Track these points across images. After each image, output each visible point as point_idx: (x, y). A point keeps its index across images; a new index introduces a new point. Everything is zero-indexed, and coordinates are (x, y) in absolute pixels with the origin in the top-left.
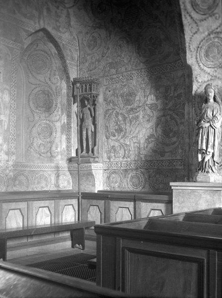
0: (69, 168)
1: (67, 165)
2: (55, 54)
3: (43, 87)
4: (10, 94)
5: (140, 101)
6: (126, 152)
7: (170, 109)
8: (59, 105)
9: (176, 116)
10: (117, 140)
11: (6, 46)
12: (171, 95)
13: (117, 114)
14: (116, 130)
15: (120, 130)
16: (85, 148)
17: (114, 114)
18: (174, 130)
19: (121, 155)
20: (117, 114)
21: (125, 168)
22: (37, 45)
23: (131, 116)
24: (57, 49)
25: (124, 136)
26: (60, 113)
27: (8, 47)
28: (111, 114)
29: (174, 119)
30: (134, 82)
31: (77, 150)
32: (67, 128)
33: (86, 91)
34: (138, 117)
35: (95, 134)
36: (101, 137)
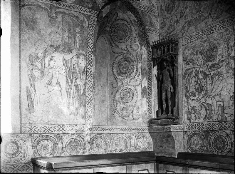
0: (149, 130)
1: (147, 127)
2: (135, 21)
3: (125, 55)
4: (86, 59)
5: (222, 54)
6: (208, 112)
8: (140, 70)
10: (198, 100)
11: (83, 14)
14: (196, 89)
15: (200, 90)
16: (165, 109)
17: (194, 73)
22: (118, 15)
23: (212, 73)
24: (136, 16)
25: (205, 95)
26: (140, 77)
27: (84, 15)
28: (190, 74)
30: (215, 35)
31: (157, 112)
32: (146, 92)
33: (164, 52)
34: (220, 74)
35: (174, 95)
36: (181, 96)
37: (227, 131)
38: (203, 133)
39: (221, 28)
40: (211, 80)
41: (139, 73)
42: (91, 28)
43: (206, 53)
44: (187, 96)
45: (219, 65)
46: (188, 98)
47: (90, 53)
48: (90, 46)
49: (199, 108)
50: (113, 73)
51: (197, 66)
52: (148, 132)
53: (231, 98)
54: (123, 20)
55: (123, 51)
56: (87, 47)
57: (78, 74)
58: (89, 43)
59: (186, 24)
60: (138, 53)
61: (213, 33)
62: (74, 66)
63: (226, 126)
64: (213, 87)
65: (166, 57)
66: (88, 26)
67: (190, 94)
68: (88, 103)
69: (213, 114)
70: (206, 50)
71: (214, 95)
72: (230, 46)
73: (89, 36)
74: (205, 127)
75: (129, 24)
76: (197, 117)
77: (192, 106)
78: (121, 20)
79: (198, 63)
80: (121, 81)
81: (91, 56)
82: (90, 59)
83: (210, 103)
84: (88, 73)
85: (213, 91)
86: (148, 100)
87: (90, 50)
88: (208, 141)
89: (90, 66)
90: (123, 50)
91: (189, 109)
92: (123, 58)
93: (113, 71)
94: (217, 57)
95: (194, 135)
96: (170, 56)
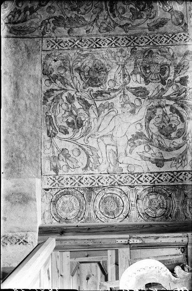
5: (114, 81)
7: (168, 98)
10: (72, 140)
14: (68, 123)
15: (77, 124)
17: (64, 99)
18: (178, 127)
19: (79, 164)
23: (98, 103)
28: (57, 97)
29: (177, 112)
30: (103, 52)
34: (111, 107)
37: (123, 188)
38: (82, 192)
39: (113, 46)
40: (96, 113)
43: (89, 72)
44: (50, 132)
45: (109, 94)
49: (74, 152)
51: (70, 88)
53: (129, 143)
59: (51, 20)
63: (122, 180)
64: (99, 124)
67: (57, 129)
71: (101, 134)
72: (127, 73)
74: (86, 182)
79: (72, 84)
83: (95, 145)
85: (100, 129)
88: (92, 203)
91: (53, 153)
94: (107, 83)
95: (64, 194)
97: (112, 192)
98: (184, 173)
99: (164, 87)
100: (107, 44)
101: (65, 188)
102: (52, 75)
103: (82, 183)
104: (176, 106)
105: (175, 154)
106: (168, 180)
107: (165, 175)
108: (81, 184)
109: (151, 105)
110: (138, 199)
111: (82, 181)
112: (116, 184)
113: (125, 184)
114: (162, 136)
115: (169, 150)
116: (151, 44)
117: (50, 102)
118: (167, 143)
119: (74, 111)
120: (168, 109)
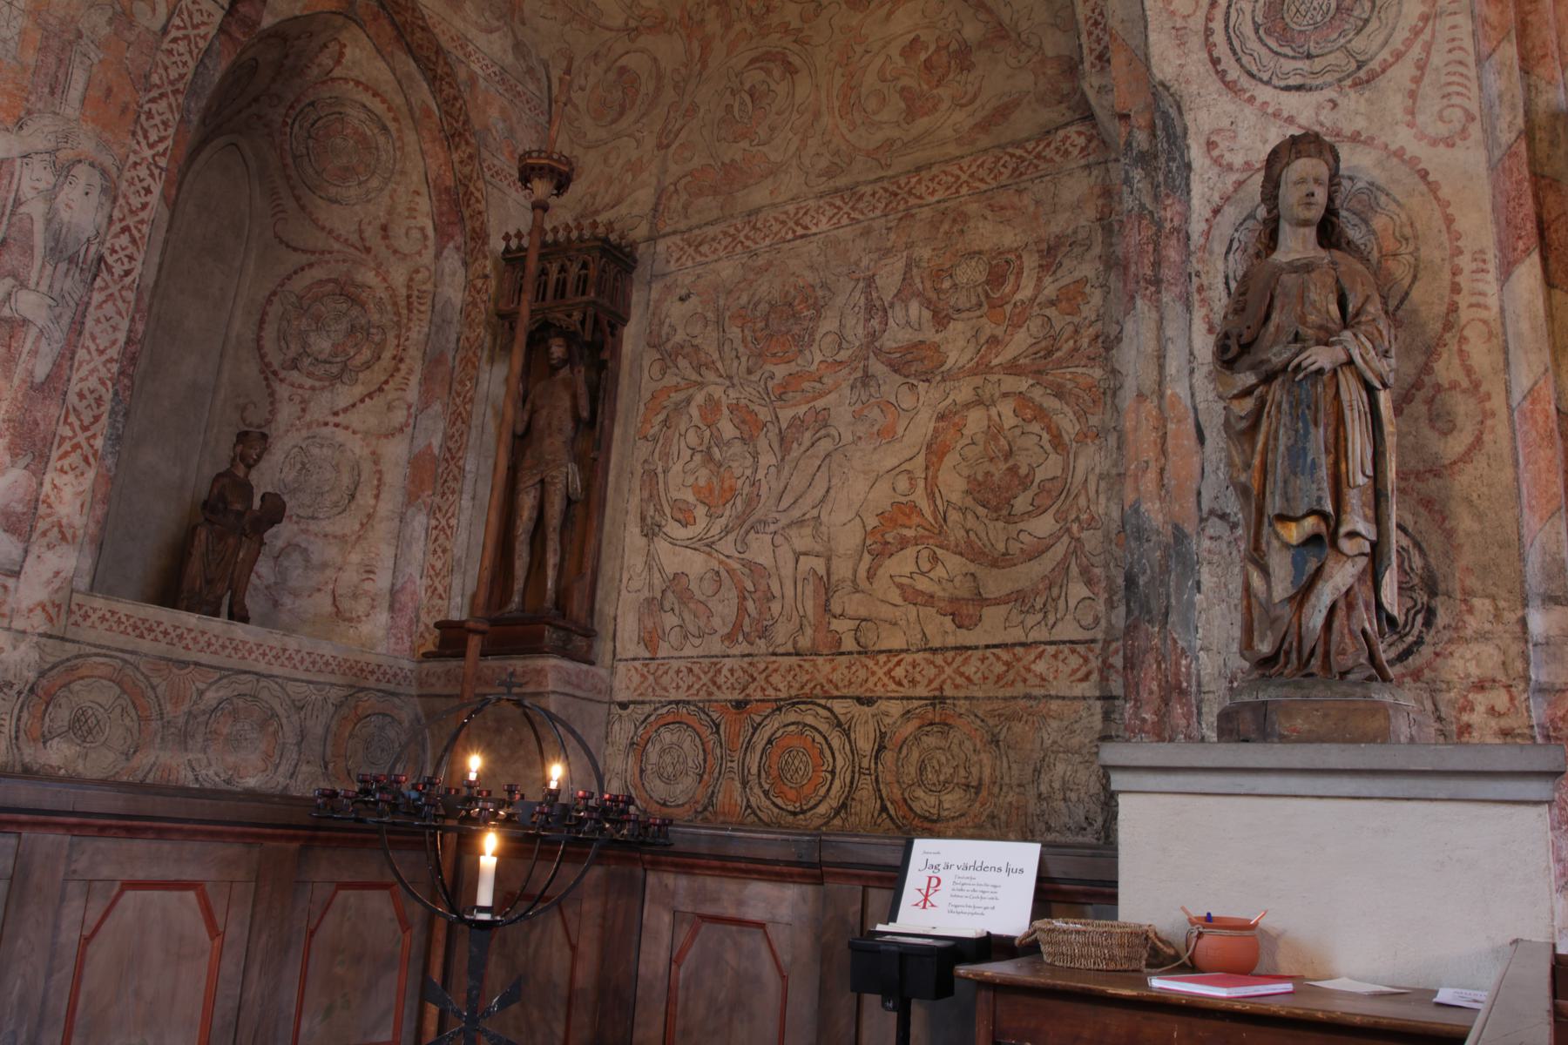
0: (421, 685)
3: (344, 267)
4: (111, 193)
6: (750, 605)
7: (1013, 368)
8: (414, 353)
9: (1051, 403)
10: (707, 546)
12: (1018, 297)
13: (712, 406)
14: (697, 490)
17: (694, 412)
19: (716, 622)
20: (712, 406)
21: (737, 696)
23: (786, 415)
25: (742, 519)
26: (413, 394)
29: (1041, 414)
32: (431, 476)
34: (822, 420)
39: (845, 221)
40: (776, 446)
41: (411, 371)
42: (182, 47)
43: (766, 319)
44: (649, 521)
46: (651, 531)
47: (143, 172)
48: (153, 137)
49: (705, 584)
50: (260, 348)
52: (414, 691)
53: (868, 542)
54: (367, 88)
55: (336, 246)
56: (134, 134)
57: (38, 263)
58: (150, 115)
59: (683, 181)
60: (417, 271)
61: (802, 237)
62: (22, 209)
64: (782, 485)
65: (570, 316)
66: (165, 31)
68: (67, 446)
69: (776, 615)
70: (764, 307)
72: (878, 303)
73: (155, 79)
75: (395, 119)
76: (692, 628)
77: (670, 571)
78: (358, 83)
79: (719, 365)
80: (297, 399)
81: (148, 191)
82: (136, 202)
83: (764, 559)
84: (104, 274)
85: (784, 504)
86: (434, 523)
87: (148, 153)
89: (124, 240)
90: (337, 239)
91: (651, 586)
92: (329, 280)
93: (259, 339)
94: (816, 345)
96: (591, 311)
97: (799, 718)
98: (1051, 649)
99: (999, 332)
100: (824, 220)
101: (670, 703)
102: (669, 346)
103: (719, 688)
104: (1037, 394)
105: (1027, 574)
106: (992, 678)
107: (983, 660)
108: (714, 689)
109: (949, 401)
110: (882, 748)
111: (721, 680)
112: (818, 691)
113: (845, 692)
114: (981, 511)
115: (1001, 561)
116: (964, 190)
117: (657, 428)
118: (996, 535)
119: (716, 450)
120: (1006, 409)
